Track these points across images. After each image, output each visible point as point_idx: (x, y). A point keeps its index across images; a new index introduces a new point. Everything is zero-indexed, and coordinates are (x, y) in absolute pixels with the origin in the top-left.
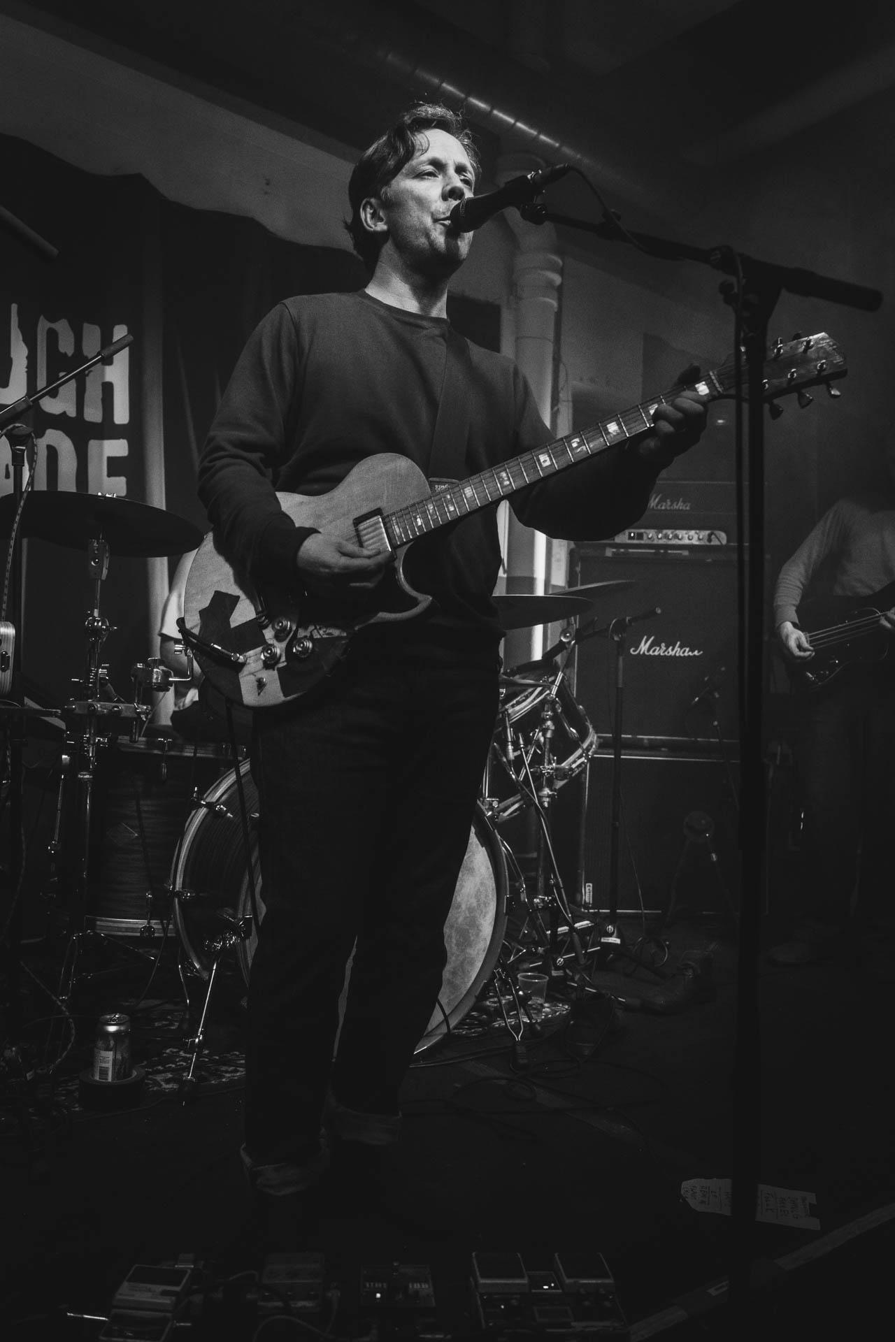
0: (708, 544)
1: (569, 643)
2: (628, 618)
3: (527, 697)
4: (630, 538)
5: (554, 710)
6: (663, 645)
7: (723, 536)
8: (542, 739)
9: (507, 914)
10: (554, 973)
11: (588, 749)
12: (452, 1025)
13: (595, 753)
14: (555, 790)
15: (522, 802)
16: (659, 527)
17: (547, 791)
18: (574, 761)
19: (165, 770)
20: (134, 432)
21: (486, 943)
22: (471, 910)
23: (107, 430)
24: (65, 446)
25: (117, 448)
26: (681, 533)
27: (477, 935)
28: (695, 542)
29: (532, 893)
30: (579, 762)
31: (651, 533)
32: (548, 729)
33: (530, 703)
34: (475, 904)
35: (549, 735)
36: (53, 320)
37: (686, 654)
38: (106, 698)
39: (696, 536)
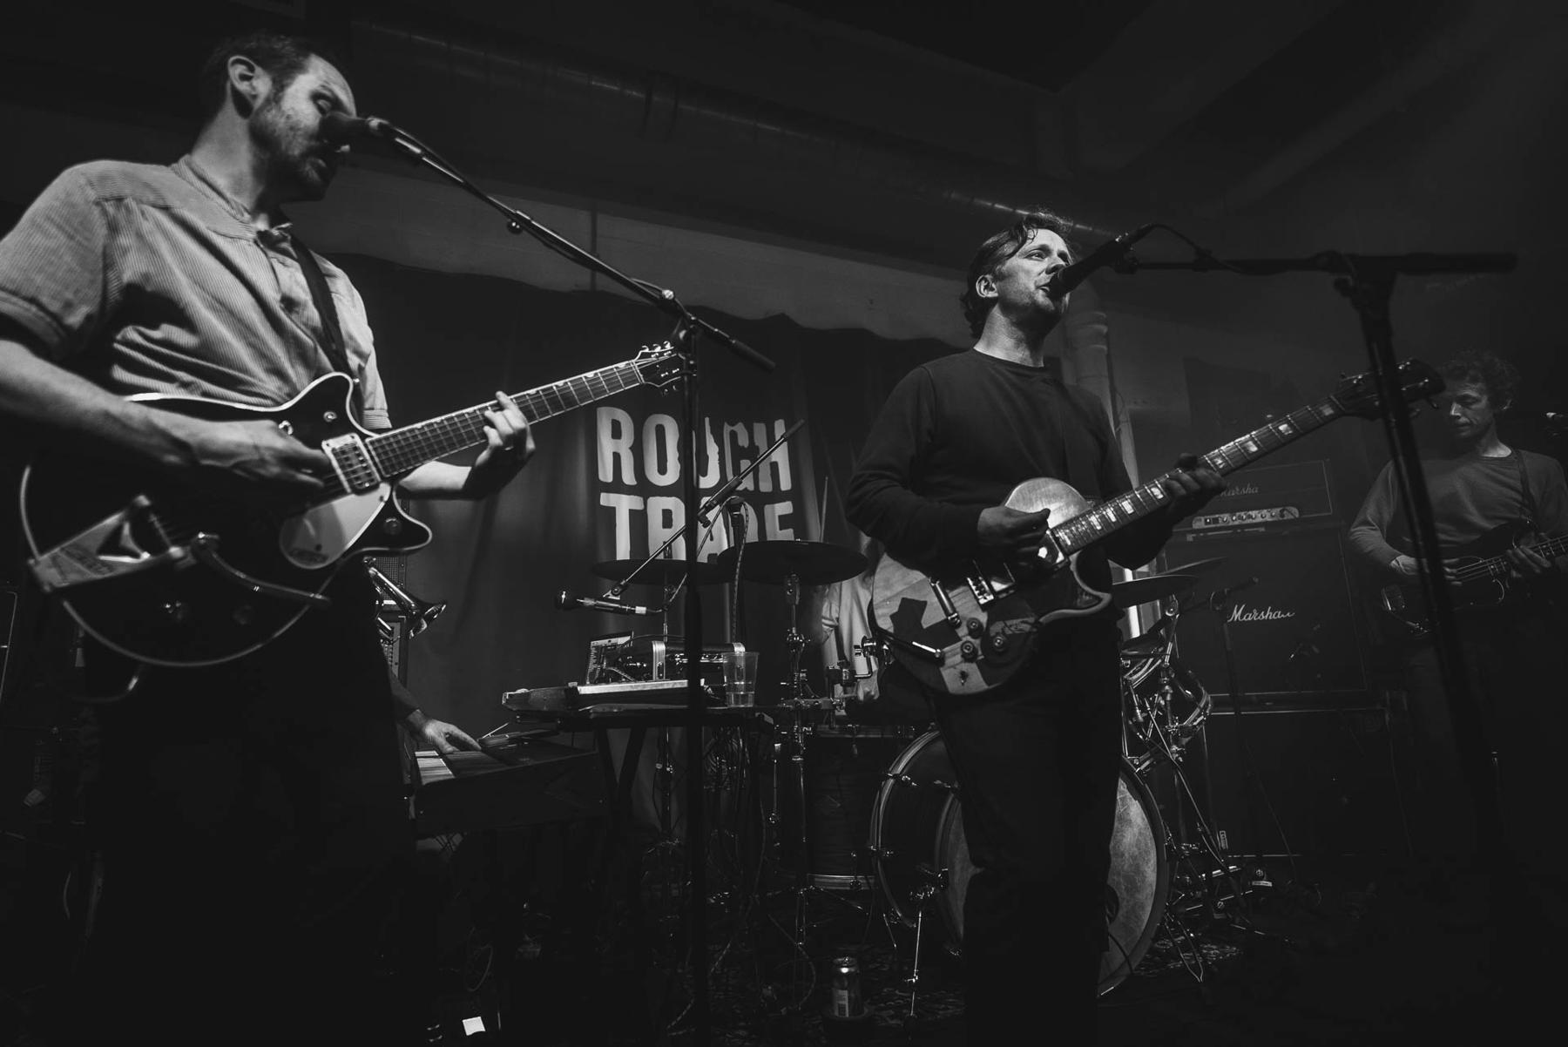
0: (1281, 519)
1: (1174, 616)
2: (1226, 590)
3: (1142, 667)
4: (1206, 523)
5: (1169, 676)
6: (1255, 611)
7: (1295, 511)
8: (1162, 702)
9: (1167, 861)
10: (1217, 916)
11: (1205, 708)
12: (1133, 968)
13: (1211, 711)
14: (1182, 746)
15: (1152, 759)
16: (1232, 512)
17: (1175, 748)
18: (1195, 719)
19: (856, 751)
20: (795, 495)
21: (1152, 889)
22: (1134, 858)
23: (776, 496)
24: (748, 512)
25: (785, 508)
26: (1253, 513)
27: (1143, 881)
28: (1268, 519)
29: (1178, 842)
30: (1199, 720)
31: (1226, 517)
32: (1167, 692)
33: (1145, 672)
34: (1137, 853)
35: (1168, 698)
36: (733, 425)
37: (1279, 617)
38: (807, 696)
39: (1268, 515)
